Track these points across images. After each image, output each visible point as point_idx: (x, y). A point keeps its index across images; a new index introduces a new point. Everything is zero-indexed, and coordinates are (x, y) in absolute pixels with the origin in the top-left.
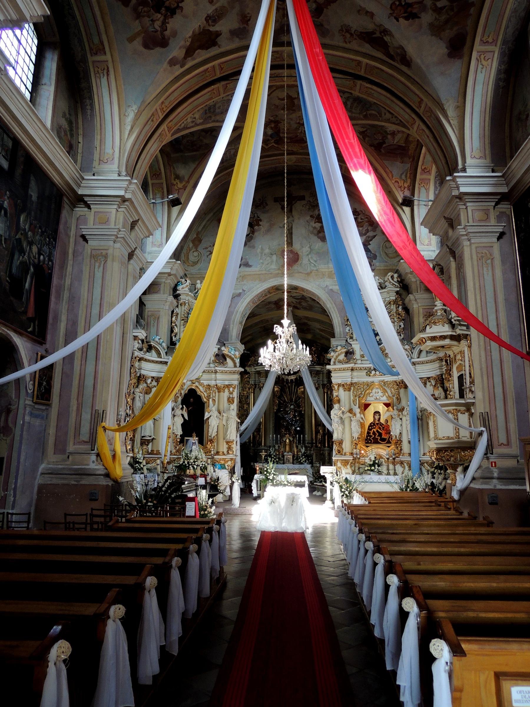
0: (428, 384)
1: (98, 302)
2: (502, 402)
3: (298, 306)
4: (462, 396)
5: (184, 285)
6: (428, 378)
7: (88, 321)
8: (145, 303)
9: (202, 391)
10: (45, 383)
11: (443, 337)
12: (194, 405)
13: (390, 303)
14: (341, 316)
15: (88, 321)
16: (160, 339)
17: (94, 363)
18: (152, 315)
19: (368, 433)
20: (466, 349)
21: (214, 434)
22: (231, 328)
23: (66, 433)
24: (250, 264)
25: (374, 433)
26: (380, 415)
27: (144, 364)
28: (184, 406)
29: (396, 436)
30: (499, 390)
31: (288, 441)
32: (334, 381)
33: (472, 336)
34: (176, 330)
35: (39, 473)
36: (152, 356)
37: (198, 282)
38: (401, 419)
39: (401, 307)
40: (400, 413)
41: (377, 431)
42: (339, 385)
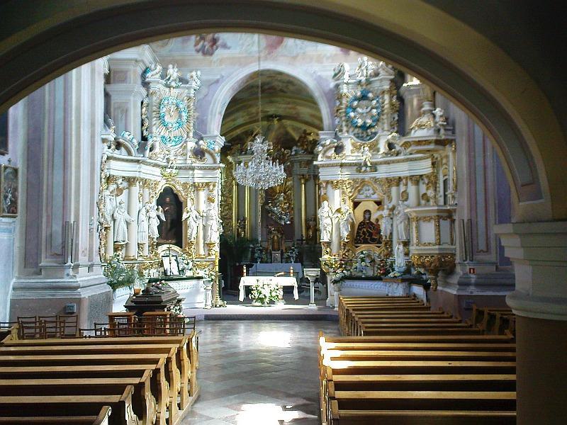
0: (421, 182)
1: (62, 105)
2: (484, 210)
3: (285, 90)
4: (445, 203)
5: (154, 72)
6: (421, 176)
7: (52, 126)
8: (111, 93)
9: (178, 188)
10: (10, 195)
11: (428, 142)
12: (172, 204)
13: (384, 92)
14: (331, 107)
15: (52, 126)
16: (131, 136)
17: (62, 172)
18: (119, 108)
19: (358, 232)
20: (451, 154)
21: (194, 235)
22: (209, 120)
23: (38, 245)
24: (229, 44)
25: (364, 233)
26: (370, 214)
27: (112, 163)
28: (160, 207)
29: (386, 237)
30: (481, 198)
31: (276, 238)
32: (322, 178)
33: (457, 141)
34: (146, 124)
35: (11, 287)
36: (122, 154)
37: (171, 66)
38: (392, 219)
39: (395, 97)
40: (391, 213)
41: (367, 231)
42: (327, 182)
